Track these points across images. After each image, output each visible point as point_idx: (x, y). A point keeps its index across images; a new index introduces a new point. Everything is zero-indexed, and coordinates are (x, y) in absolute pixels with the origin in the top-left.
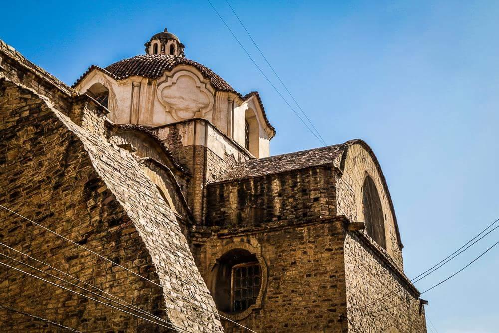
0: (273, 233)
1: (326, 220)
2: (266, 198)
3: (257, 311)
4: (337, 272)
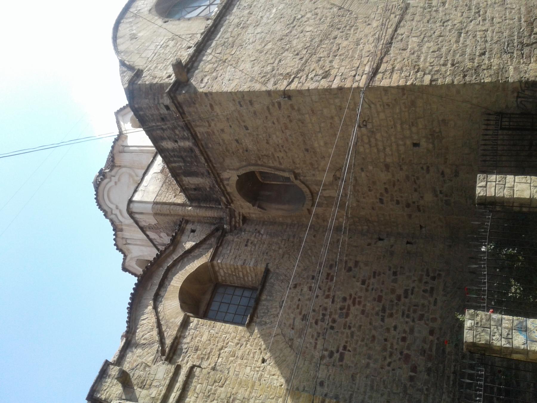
0: (212, 159)
1: (179, 112)
2: (184, 154)
3: (296, 176)
4: (234, 100)
